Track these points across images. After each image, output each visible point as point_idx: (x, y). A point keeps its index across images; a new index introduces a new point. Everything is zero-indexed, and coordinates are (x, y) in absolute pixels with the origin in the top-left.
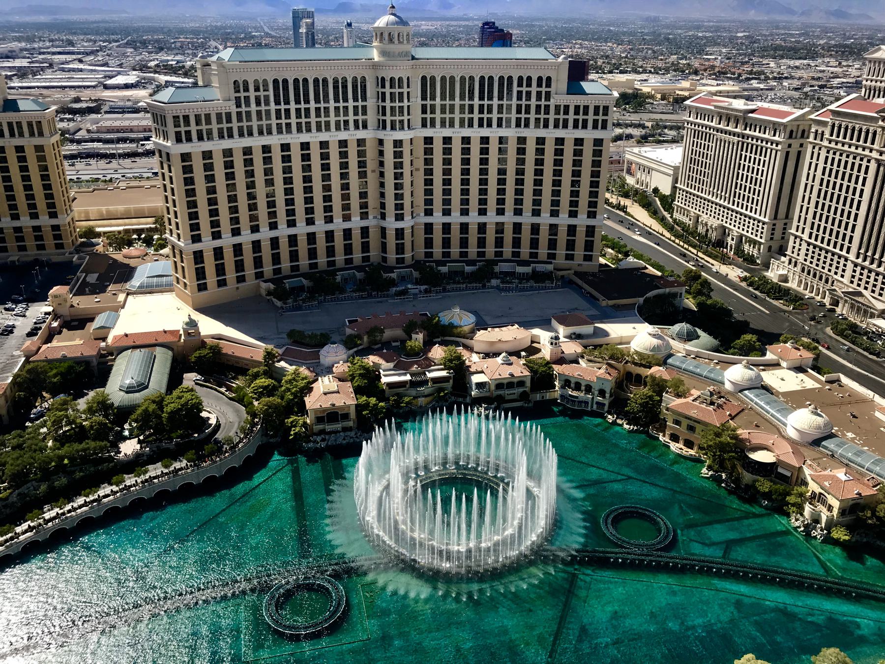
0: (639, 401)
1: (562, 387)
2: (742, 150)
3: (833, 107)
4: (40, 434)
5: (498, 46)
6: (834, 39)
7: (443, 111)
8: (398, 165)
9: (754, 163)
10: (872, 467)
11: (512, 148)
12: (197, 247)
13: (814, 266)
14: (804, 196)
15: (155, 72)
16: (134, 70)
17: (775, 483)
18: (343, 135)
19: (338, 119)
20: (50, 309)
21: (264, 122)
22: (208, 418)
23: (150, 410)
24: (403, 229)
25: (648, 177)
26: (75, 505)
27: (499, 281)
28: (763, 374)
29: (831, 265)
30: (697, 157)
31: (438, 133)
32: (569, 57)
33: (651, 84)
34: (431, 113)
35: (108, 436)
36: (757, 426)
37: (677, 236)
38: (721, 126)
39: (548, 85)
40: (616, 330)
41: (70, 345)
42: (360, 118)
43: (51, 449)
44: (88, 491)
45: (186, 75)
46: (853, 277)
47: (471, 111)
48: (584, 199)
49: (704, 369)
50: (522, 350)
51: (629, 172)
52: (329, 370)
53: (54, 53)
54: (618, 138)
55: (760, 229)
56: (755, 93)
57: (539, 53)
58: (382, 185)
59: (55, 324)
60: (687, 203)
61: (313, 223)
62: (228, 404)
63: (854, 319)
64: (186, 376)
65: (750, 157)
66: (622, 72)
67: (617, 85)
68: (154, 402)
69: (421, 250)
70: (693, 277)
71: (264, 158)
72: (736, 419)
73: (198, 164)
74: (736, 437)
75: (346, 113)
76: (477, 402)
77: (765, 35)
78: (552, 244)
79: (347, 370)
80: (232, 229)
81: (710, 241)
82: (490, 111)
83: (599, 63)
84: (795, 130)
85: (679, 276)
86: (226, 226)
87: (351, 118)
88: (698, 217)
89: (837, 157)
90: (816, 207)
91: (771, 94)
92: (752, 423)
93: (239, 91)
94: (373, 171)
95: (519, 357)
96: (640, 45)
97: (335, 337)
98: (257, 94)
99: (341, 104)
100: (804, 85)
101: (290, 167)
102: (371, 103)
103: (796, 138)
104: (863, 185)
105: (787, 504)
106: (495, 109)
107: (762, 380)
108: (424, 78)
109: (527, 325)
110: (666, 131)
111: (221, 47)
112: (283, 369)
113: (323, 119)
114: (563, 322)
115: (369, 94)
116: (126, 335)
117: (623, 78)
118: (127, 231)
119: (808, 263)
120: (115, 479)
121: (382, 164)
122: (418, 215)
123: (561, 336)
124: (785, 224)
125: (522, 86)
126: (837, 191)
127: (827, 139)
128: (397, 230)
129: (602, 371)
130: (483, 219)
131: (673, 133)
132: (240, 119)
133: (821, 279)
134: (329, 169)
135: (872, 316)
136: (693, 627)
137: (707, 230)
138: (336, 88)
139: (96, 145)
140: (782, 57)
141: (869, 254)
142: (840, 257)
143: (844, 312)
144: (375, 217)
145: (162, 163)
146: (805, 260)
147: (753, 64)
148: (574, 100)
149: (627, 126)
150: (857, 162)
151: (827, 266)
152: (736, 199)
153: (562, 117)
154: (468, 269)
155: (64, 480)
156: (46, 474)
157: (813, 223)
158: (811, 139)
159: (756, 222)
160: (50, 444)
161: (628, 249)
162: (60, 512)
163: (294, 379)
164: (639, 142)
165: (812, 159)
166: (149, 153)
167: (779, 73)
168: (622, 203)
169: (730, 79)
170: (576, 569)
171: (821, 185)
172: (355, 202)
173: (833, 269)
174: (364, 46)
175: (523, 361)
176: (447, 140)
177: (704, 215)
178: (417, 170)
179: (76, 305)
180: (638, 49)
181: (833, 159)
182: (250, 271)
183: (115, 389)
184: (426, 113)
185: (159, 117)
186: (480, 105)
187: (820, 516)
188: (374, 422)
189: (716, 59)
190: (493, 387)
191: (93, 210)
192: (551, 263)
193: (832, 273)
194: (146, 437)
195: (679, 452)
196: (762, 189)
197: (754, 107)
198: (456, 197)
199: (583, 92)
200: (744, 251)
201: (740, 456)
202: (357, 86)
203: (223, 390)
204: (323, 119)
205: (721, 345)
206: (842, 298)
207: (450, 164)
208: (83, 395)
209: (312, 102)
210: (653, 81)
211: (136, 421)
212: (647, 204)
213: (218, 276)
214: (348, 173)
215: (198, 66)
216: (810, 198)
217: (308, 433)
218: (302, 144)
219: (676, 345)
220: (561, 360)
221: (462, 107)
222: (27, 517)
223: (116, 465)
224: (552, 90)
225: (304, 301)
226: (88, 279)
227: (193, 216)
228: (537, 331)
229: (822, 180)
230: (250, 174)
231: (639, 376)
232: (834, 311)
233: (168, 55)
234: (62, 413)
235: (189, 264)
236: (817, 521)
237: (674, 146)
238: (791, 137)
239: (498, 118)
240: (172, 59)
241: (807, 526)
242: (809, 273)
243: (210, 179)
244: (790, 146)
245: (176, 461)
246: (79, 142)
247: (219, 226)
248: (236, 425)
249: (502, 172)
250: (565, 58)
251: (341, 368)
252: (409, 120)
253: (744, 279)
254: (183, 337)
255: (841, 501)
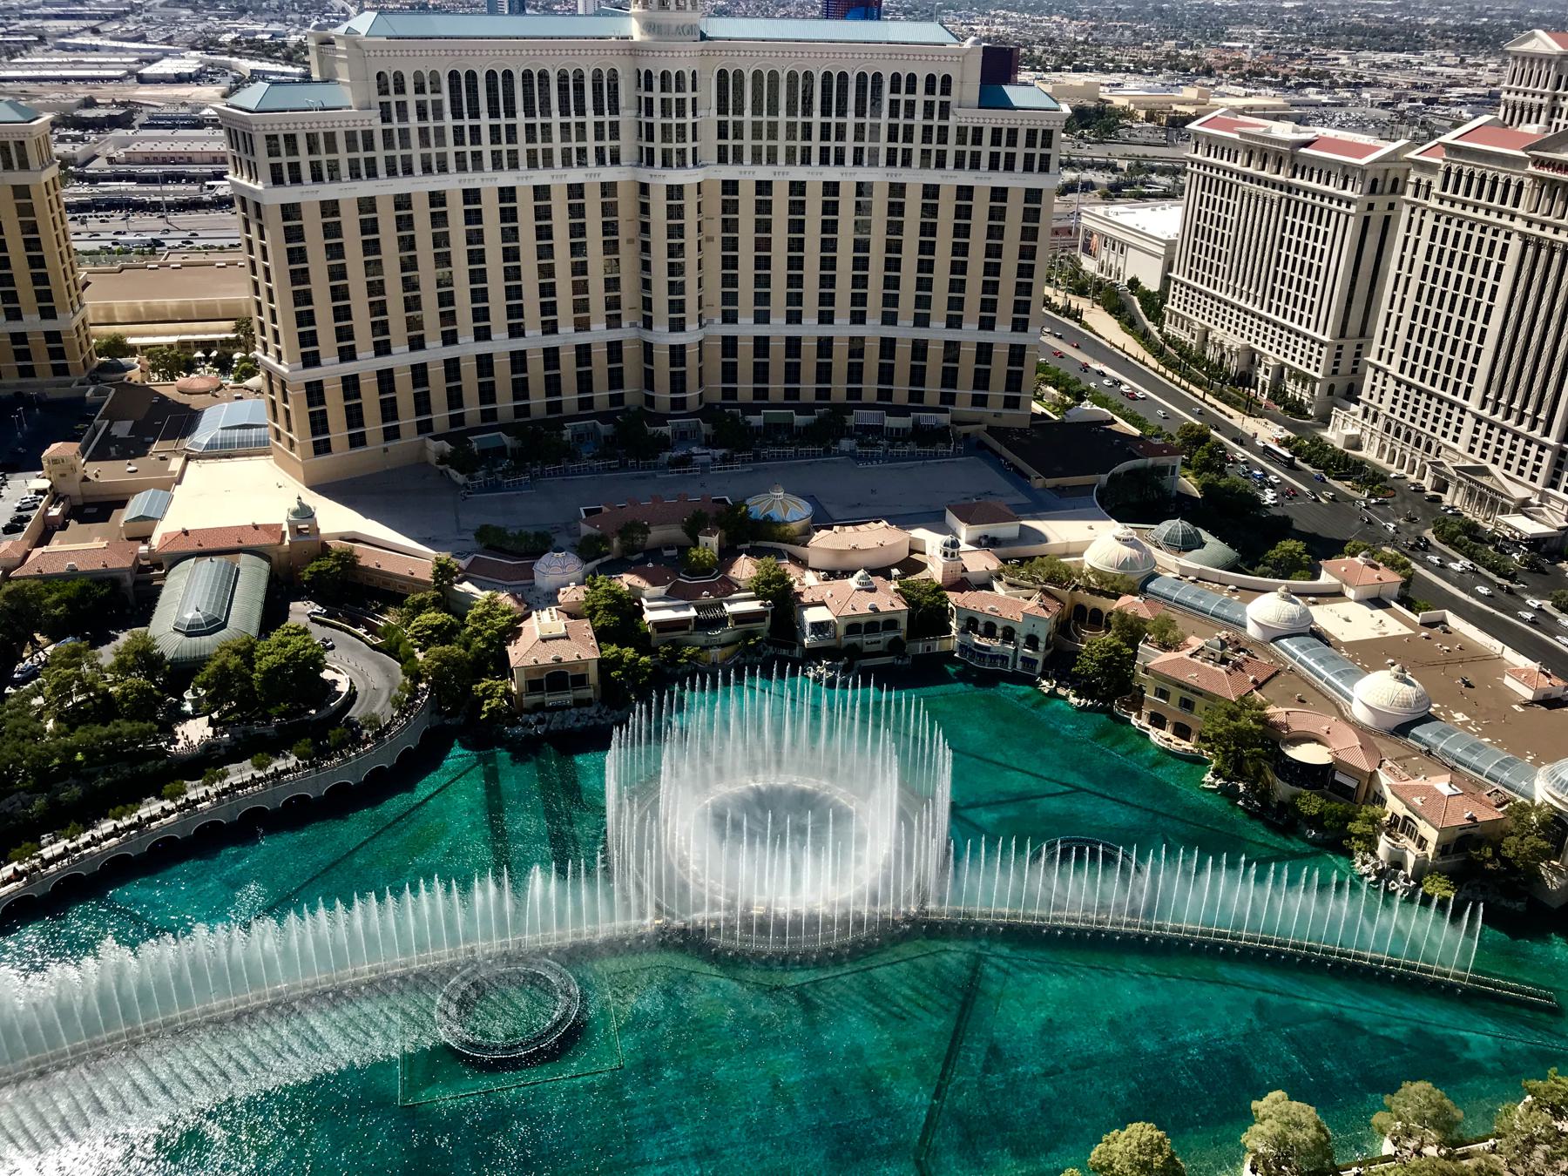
0: (1097, 656)
1: (963, 631)
2: (1287, 214)
3: (1448, 138)
4: (31, 708)
5: (855, 18)
6: (1452, 16)
7: (757, 134)
8: (676, 231)
9: (1308, 237)
10: (1496, 773)
11: (879, 203)
12: (313, 374)
13: (1406, 421)
14: (1393, 297)
15: (233, 53)
16: (194, 48)
17: (1329, 800)
18: (576, 175)
19: (567, 145)
20: (45, 484)
21: (433, 150)
22: (335, 682)
23: (231, 666)
24: (683, 347)
25: (1121, 260)
26: (98, 834)
27: (854, 442)
28: (1313, 610)
29: (1436, 420)
30: (1207, 225)
31: (747, 174)
32: (984, 40)
33: (1127, 92)
34: (735, 137)
35: (154, 711)
36: (1301, 701)
37: (1170, 365)
38: (1250, 170)
39: (946, 91)
40: (1059, 532)
41: (82, 549)
42: (607, 144)
43: (51, 734)
44: (119, 809)
45: (288, 59)
46: (1474, 440)
47: (807, 136)
48: (1006, 296)
49: (1212, 600)
50: (894, 566)
51: (1087, 249)
52: (550, 598)
53: (47, 17)
54: (1069, 188)
55: (1315, 355)
56: (1313, 111)
57: (929, 32)
58: (646, 266)
59: (55, 512)
60: (1188, 307)
61: (522, 334)
62: (370, 657)
63: (1473, 514)
64: (292, 605)
65: (1301, 226)
66: (1077, 69)
67: (1069, 92)
68: (237, 652)
69: (716, 385)
70: (1197, 439)
71: (433, 214)
72: (1265, 689)
73: (312, 225)
74: (1264, 720)
75: (581, 136)
76: (814, 655)
77: (1333, 7)
78: (950, 378)
79: (582, 598)
80: (376, 344)
81: (1227, 374)
82: (841, 136)
83: (1037, 53)
84: (1380, 178)
85: (1171, 437)
86: (363, 339)
87: (591, 144)
88: (1207, 331)
89: (1453, 229)
90: (1414, 317)
91: (1341, 114)
92: (1293, 695)
93: (386, 92)
94: (630, 241)
95: (888, 577)
96: (1111, 20)
97: (560, 540)
98: (421, 97)
99: (573, 119)
100: (1398, 98)
101: (480, 232)
102: (627, 117)
103: (1382, 193)
104: (1497, 278)
105: (1350, 835)
106: (850, 132)
107: (1312, 621)
108: (722, 74)
109: (903, 520)
110: (1154, 176)
111: (353, 10)
112: (468, 595)
113: (539, 146)
114: (967, 518)
115: (622, 102)
116: (186, 533)
117: (1078, 80)
118: (184, 345)
119: (1396, 416)
120: (168, 788)
121: (645, 228)
122: (711, 321)
123: (962, 542)
124: (1360, 346)
125: (898, 92)
126: (1450, 289)
127: (1437, 196)
128: (672, 347)
129: (1033, 603)
130: (826, 330)
131: (1166, 181)
132: (388, 144)
133: (1418, 443)
134: (550, 237)
135: (1505, 510)
136: (1184, 1046)
137: (1223, 356)
138: (563, 89)
139: (124, 185)
140: (1361, 47)
141: (1503, 400)
142: (1452, 406)
143: (1457, 503)
144: (633, 325)
145: (246, 222)
146: (1392, 410)
147: (1310, 59)
148: (991, 119)
149: (1085, 167)
150: (1488, 237)
151: (1429, 422)
152: (1275, 302)
153: (969, 148)
154: (800, 420)
155: (77, 790)
156: (44, 779)
157: (1408, 346)
158: (1409, 196)
159: (1308, 342)
160: (50, 725)
161: (1082, 387)
162: (70, 846)
163: (488, 613)
164: (1105, 196)
165: (1409, 230)
166: (223, 203)
167: (1355, 76)
168: (1074, 306)
169: (1270, 84)
170: (981, 947)
171: (1424, 277)
172: (597, 295)
173: (1440, 427)
174: (614, 14)
175: (894, 585)
176: (764, 187)
177: (1218, 329)
178: (710, 239)
179: (92, 478)
180: (1107, 27)
181: (1446, 231)
182: (407, 419)
183: (169, 626)
184: (726, 137)
185: (240, 137)
186: (823, 124)
187: (1403, 855)
188: (631, 690)
189: (1244, 47)
190: (841, 631)
191: (120, 306)
192: (946, 411)
193: (1438, 434)
194: (224, 715)
195: (1164, 744)
196: (1320, 284)
197: (1309, 137)
198: (779, 289)
199: (1006, 105)
200: (1286, 393)
201: (1271, 753)
202: (601, 86)
203: (361, 631)
204: (539, 146)
205: (1242, 560)
206: (1452, 478)
207: (768, 230)
208: (109, 639)
209: (520, 114)
210: (1132, 86)
211: (205, 686)
212: (1116, 306)
213: (350, 427)
214: (584, 244)
215: (312, 43)
216: (1403, 300)
217: (514, 710)
218: (501, 190)
219: (1168, 562)
220: (962, 583)
221: (791, 127)
222: (11, 855)
223: (169, 765)
224: (953, 98)
225: (505, 473)
226: (114, 431)
227: (306, 319)
228: (919, 533)
229: (1426, 268)
230: (408, 243)
231: (1097, 613)
232: (1438, 500)
233: (256, 22)
234: (71, 671)
235: (297, 406)
236: (1398, 864)
237: (1167, 203)
238: (1372, 191)
239: (856, 149)
240: (263, 30)
241: (1381, 874)
242: (1397, 434)
243: (335, 251)
244: (1371, 207)
245: (277, 757)
246: (93, 180)
247: (351, 338)
248: (385, 695)
249: (861, 246)
250: (975, 42)
251: (572, 594)
252: (695, 150)
253: (1285, 443)
254: (288, 537)
255: (1441, 830)
